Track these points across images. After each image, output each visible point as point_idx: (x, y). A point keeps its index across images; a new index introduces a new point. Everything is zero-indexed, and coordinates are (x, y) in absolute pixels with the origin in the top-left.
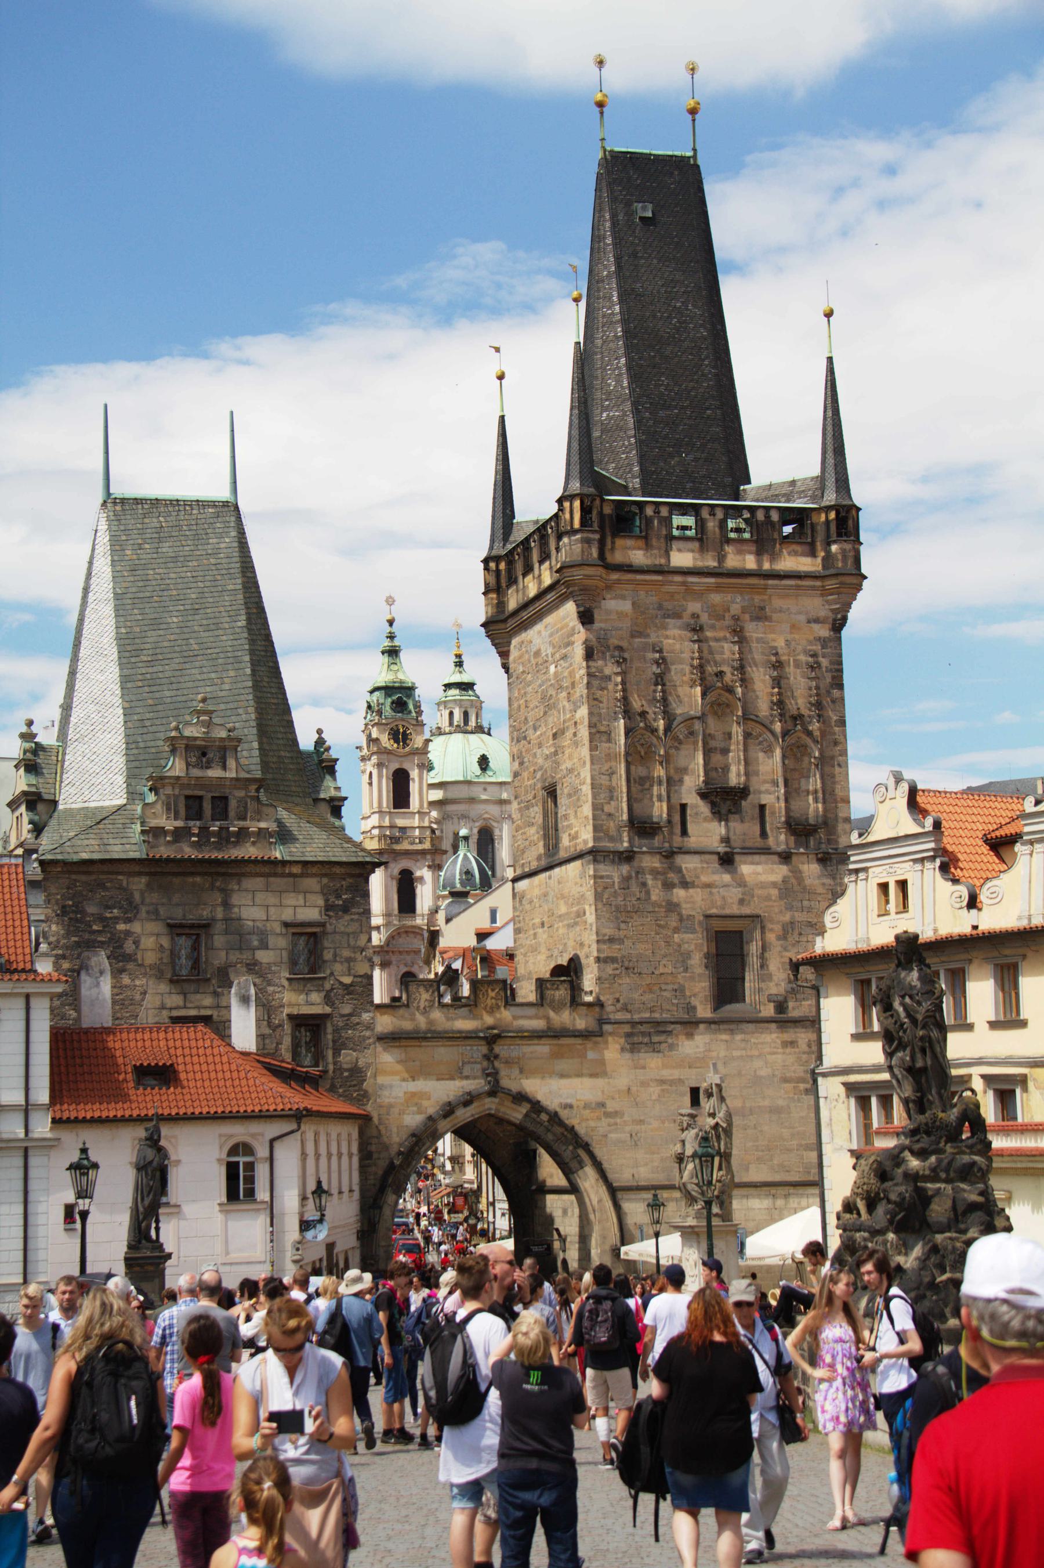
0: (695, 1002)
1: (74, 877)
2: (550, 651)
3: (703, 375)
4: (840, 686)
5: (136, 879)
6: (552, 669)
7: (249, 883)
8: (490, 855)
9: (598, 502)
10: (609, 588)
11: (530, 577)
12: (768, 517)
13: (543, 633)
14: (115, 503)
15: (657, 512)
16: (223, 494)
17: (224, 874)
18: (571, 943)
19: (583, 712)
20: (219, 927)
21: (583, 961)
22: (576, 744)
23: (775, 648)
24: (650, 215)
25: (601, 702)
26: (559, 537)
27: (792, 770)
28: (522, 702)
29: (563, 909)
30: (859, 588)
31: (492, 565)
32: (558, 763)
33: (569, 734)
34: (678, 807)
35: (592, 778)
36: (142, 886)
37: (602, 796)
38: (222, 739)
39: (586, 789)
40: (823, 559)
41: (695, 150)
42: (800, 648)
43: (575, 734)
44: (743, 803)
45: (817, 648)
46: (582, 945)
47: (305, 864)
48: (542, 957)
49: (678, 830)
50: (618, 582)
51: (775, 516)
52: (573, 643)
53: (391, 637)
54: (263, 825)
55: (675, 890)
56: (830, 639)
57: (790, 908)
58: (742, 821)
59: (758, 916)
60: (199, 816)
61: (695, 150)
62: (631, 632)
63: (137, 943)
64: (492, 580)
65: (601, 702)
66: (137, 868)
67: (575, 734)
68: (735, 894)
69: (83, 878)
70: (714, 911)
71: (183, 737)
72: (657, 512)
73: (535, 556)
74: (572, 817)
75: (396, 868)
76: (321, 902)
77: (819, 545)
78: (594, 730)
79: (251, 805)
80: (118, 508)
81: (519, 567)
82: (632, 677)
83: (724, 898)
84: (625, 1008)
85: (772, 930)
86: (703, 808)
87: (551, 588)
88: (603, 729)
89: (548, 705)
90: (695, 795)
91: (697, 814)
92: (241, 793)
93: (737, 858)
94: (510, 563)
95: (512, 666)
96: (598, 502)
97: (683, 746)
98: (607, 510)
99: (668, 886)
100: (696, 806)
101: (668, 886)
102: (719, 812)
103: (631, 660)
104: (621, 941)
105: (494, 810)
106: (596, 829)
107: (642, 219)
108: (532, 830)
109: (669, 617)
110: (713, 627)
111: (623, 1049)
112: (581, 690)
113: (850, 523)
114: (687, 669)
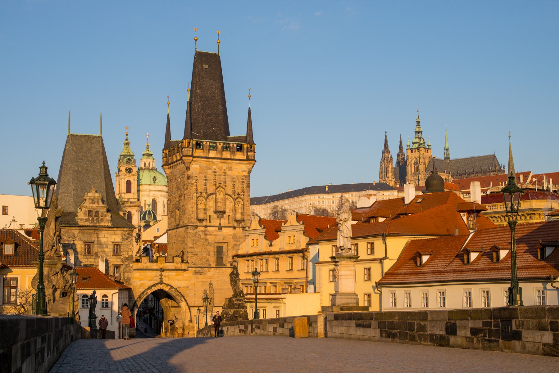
0: (211, 263)
4: (249, 187)
5: (76, 231)
6: (179, 180)
7: (103, 232)
8: (155, 205)
11: (174, 156)
12: (233, 145)
15: (206, 143)
17: (97, 230)
18: (181, 248)
20: (96, 243)
26: (182, 149)
29: (180, 239)
30: (254, 164)
31: (165, 151)
33: (183, 197)
36: (77, 232)
42: (240, 178)
43: (184, 197)
45: (244, 178)
46: (184, 248)
51: (235, 145)
56: (247, 176)
57: (235, 241)
58: (224, 219)
60: (91, 215)
68: (222, 237)
70: (216, 241)
72: (206, 143)
73: (176, 151)
74: (183, 217)
76: (121, 237)
79: (105, 213)
81: (172, 153)
82: (198, 184)
84: (194, 264)
86: (215, 216)
87: (179, 160)
92: (102, 210)
98: (194, 143)
99: (206, 235)
100: (213, 216)
101: (206, 235)
105: (158, 194)
109: (208, 169)
110: (219, 172)
111: (193, 274)
113: (253, 148)
114: (212, 182)
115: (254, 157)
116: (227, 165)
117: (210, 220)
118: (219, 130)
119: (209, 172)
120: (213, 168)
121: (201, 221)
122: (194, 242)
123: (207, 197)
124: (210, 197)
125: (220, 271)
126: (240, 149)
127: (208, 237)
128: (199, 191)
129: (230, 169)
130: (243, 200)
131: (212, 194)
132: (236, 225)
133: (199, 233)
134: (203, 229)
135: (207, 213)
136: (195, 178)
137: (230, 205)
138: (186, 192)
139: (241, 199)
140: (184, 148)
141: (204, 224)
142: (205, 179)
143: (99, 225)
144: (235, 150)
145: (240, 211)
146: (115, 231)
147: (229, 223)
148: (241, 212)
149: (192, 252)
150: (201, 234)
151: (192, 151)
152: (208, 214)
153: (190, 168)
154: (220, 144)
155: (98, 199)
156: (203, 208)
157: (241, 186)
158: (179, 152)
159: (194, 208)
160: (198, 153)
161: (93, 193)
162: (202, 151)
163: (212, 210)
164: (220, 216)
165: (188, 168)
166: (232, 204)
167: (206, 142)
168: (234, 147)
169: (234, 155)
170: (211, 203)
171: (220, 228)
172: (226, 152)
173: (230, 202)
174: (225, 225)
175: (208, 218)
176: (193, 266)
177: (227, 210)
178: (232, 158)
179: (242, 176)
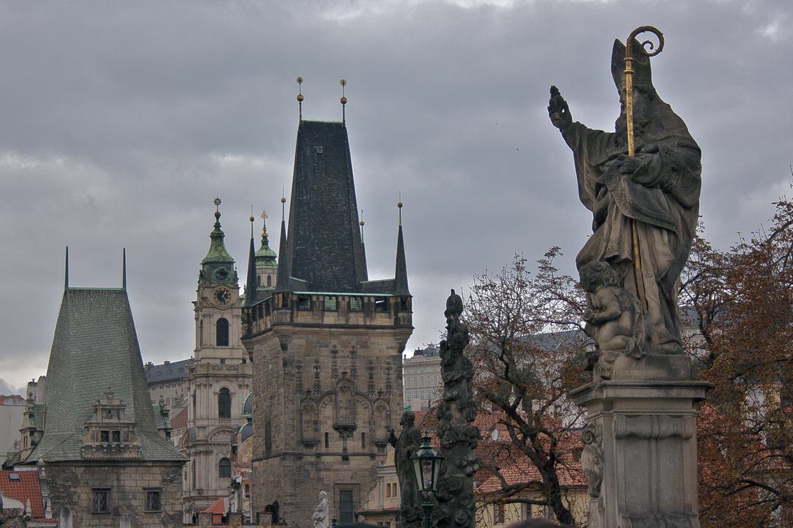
1: (52, 468)
5: (79, 468)
7: (128, 470)
10: (295, 333)
11: (261, 321)
12: (369, 300)
15: (318, 298)
16: (120, 286)
18: (275, 495)
20: (115, 489)
22: (279, 404)
23: (371, 360)
26: (273, 311)
29: (272, 479)
31: (246, 310)
33: (276, 398)
36: (81, 472)
38: (118, 406)
41: (344, 120)
44: (354, 432)
45: (391, 360)
46: (279, 496)
47: (154, 461)
49: (324, 444)
51: (373, 300)
53: (217, 226)
54: (135, 444)
56: (397, 356)
59: (359, 484)
61: (344, 120)
63: (79, 497)
64: (246, 318)
66: (79, 464)
68: (349, 474)
69: (57, 468)
71: (101, 405)
72: (318, 298)
75: (217, 387)
76: (160, 478)
80: (72, 295)
81: (258, 313)
83: (343, 476)
85: (365, 490)
86: (337, 434)
87: (270, 330)
93: (350, 458)
97: (327, 407)
98: (295, 298)
99: (319, 470)
100: (333, 433)
104: (296, 496)
106: (286, 444)
108: (261, 439)
110: (343, 351)
112: (281, 380)
113: (407, 304)
117: (327, 441)
118: (345, 270)
120: (332, 344)
121: (309, 445)
123: (320, 401)
126: (384, 307)
128: (306, 387)
129: (365, 345)
130: (388, 403)
131: (329, 393)
132: (375, 450)
133: (309, 467)
134: (313, 459)
138: (282, 390)
139: (384, 400)
141: (314, 450)
143: (119, 457)
144: (373, 309)
145: (384, 423)
146: (149, 467)
147: (363, 446)
148: (385, 425)
149: (292, 504)
150: (310, 469)
151: (292, 314)
153: (289, 347)
154: (344, 299)
155: (119, 409)
156: (313, 419)
157: (384, 377)
159: (295, 420)
160: (303, 317)
161: (108, 398)
162: (310, 313)
163: (330, 423)
164: (345, 434)
165: (284, 347)
166: (368, 412)
168: (372, 303)
169: (372, 319)
170: (327, 412)
173: (365, 408)
177: (360, 423)
178: (368, 323)
179: (388, 358)
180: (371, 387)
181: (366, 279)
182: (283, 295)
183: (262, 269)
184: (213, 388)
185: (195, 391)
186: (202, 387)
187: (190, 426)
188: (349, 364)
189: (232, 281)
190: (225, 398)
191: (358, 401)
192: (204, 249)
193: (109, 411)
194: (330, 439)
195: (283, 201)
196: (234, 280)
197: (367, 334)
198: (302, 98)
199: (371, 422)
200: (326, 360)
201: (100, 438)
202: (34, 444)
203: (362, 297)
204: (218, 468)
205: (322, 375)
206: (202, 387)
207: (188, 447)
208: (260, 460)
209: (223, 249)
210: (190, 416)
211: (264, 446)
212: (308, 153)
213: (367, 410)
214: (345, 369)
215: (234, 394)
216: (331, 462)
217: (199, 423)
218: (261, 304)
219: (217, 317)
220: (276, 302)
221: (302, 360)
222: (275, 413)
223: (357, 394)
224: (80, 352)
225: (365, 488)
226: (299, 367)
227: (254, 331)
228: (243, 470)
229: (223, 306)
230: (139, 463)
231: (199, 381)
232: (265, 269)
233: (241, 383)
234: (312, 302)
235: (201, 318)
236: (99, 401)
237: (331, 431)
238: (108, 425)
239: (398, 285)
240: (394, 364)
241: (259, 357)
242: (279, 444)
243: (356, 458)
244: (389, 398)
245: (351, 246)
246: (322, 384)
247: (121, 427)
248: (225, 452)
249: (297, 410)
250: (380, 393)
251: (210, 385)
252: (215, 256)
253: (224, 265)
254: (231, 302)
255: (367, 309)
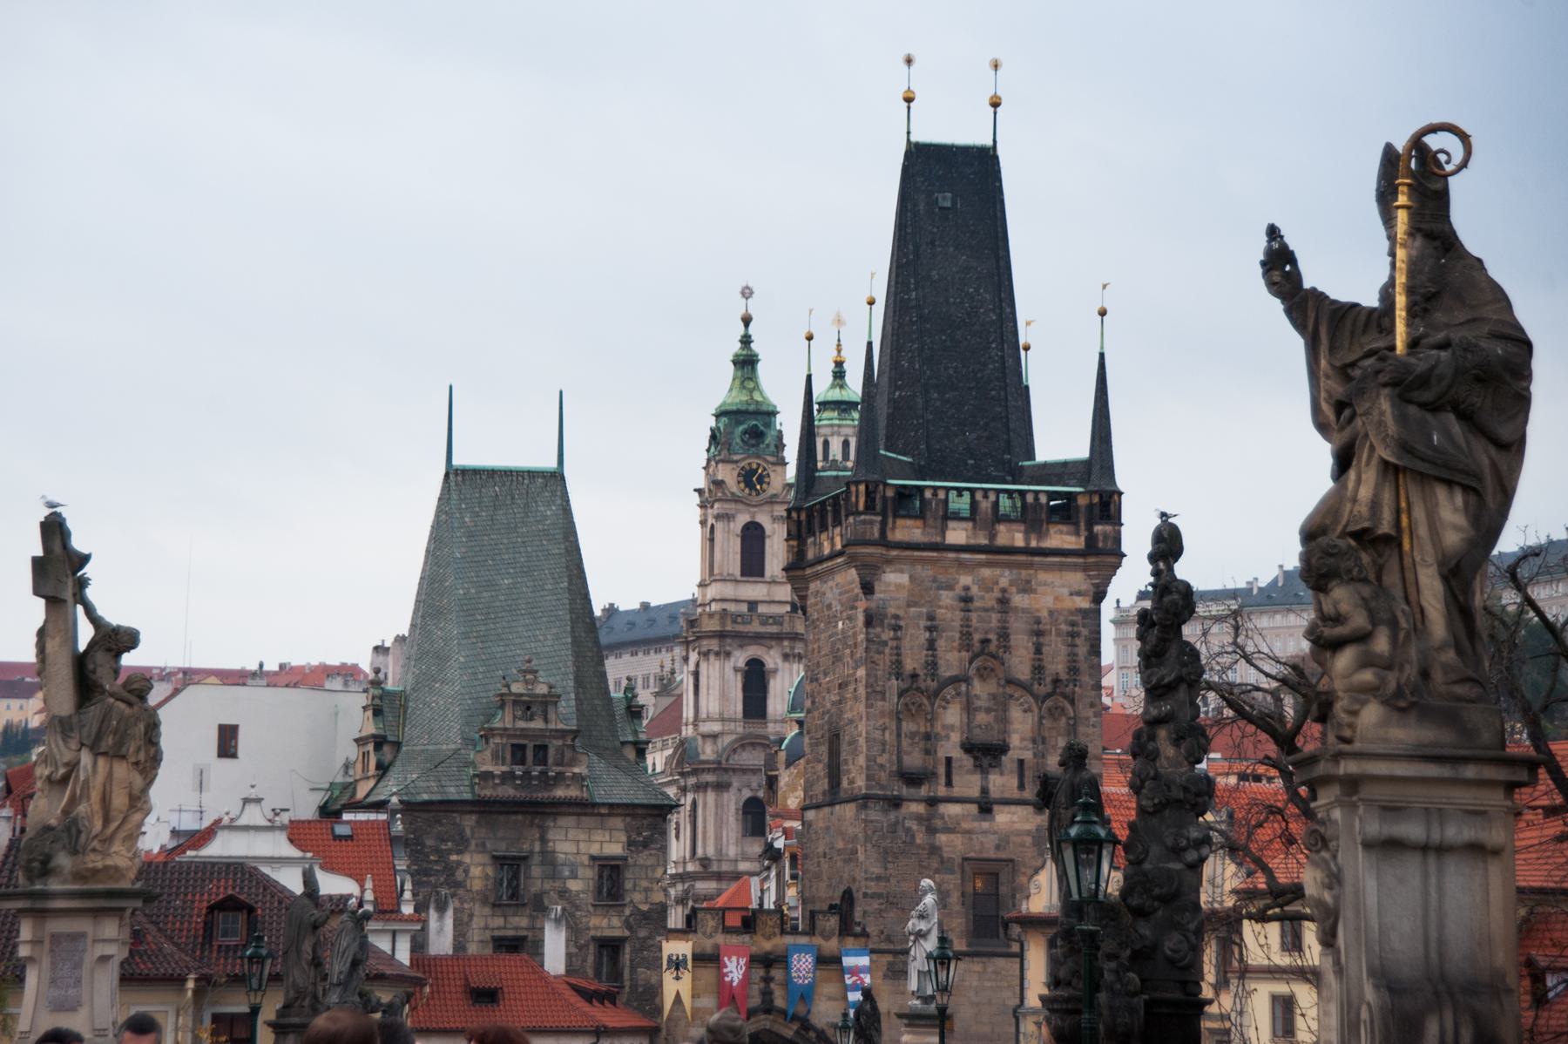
1: (416, 814)
2: (839, 608)
3: (990, 358)
5: (468, 817)
6: (840, 624)
7: (564, 821)
9: (881, 487)
10: (889, 562)
11: (824, 536)
12: (1036, 499)
13: (835, 590)
14: (456, 474)
15: (935, 494)
16: (549, 462)
17: (542, 813)
18: (846, 876)
19: (861, 672)
20: (536, 859)
21: (855, 895)
24: (948, 204)
25: (877, 665)
26: (847, 516)
27: (1050, 728)
28: (816, 646)
29: (840, 845)
30: (1119, 565)
31: (794, 515)
32: (841, 712)
33: (851, 688)
34: (944, 760)
35: (867, 733)
37: (875, 749)
38: (544, 696)
39: (862, 741)
40: (1087, 539)
42: (1061, 618)
43: (855, 690)
44: (1003, 758)
46: (854, 880)
47: (611, 806)
48: (823, 885)
49: (943, 780)
50: (898, 558)
51: (1043, 499)
52: (856, 608)
53: (746, 341)
54: (576, 770)
55: (938, 835)
59: (1012, 861)
60: (523, 762)
62: (908, 602)
63: (466, 871)
64: (794, 530)
65: (877, 665)
66: (469, 808)
67: (855, 690)
68: (991, 841)
69: (425, 815)
70: (972, 855)
71: (511, 694)
72: (935, 494)
74: (850, 762)
75: (740, 658)
76: (624, 838)
77: (1082, 525)
78: (869, 690)
80: (460, 478)
81: (817, 522)
82: (906, 643)
83: (982, 843)
84: (889, 939)
85: (1024, 873)
86: (968, 761)
87: (840, 554)
88: (878, 689)
89: (837, 659)
90: (959, 749)
91: (960, 767)
93: (996, 808)
94: (810, 517)
95: (809, 610)
96: (881, 487)
98: (890, 493)
99: (932, 831)
100: (961, 760)
101: (932, 831)
102: (981, 766)
103: (907, 627)
106: (869, 778)
107: (941, 208)
110: (982, 598)
111: (885, 976)
112: (860, 652)
113: (1112, 507)
114: (957, 635)
115: (1117, 540)
116: (1015, 572)
119: (947, 597)
121: (913, 779)
122: (886, 855)
123: (937, 693)
124: (949, 691)
125: (985, 969)
126: (1065, 512)
127: (942, 838)
128: (910, 665)
130: (1072, 702)
131: (955, 680)
133: (908, 823)
134: (919, 808)
135: (935, 752)
136: (893, 622)
137: (1021, 725)
140: (853, 514)
141: (924, 791)
142: (929, 623)
143: (546, 795)
144: (1044, 516)
146: (602, 815)
147: (1021, 786)
150: (915, 827)
151: (884, 524)
152: (942, 754)
153: (876, 588)
154: (986, 497)
156: (922, 730)
157: (1064, 650)
158: (840, 524)
160: (907, 530)
161: (527, 682)
162: (919, 523)
163: (956, 738)
164: (986, 761)
165: (868, 588)
167: (935, 489)
168: (1041, 505)
169: (1041, 535)
170: (952, 715)
171: (986, 807)
172: (1008, 525)
174: (1007, 795)
175: (942, 770)
176: (884, 946)
177: (1015, 740)
178: (1034, 544)
180: (1038, 669)
181: (1030, 453)
182: (867, 487)
183: (832, 426)
184: (733, 659)
185: (697, 665)
186: (712, 658)
187: (688, 732)
188: (994, 623)
189: (772, 448)
190: (755, 680)
191: (1011, 696)
192: (720, 387)
193: (527, 706)
194: (954, 771)
195: (871, 303)
196: (776, 447)
197: (1030, 566)
198: (912, 95)
199: (1039, 740)
200: (949, 616)
201: (508, 757)
202: (383, 769)
203: (1022, 493)
204: (740, 817)
205: (941, 644)
206: (712, 658)
207: (682, 774)
208: (817, 807)
209: (757, 387)
210: (688, 712)
211: (826, 781)
212: (922, 207)
213: (1030, 714)
214: (986, 633)
215: (775, 671)
216: (957, 816)
217: (706, 728)
218: (823, 503)
219: (743, 519)
220: (853, 499)
221: (901, 613)
222: (848, 715)
223: (1010, 682)
224: (473, 591)
225: (1023, 870)
226: (896, 628)
227: (811, 555)
228: (788, 824)
229: (755, 499)
230: (584, 808)
231: (706, 644)
232: (839, 426)
233: (788, 651)
234: (923, 500)
235: (710, 521)
236: (508, 686)
237: (957, 753)
238: (524, 733)
239: (1096, 468)
240: (1083, 627)
241: (820, 606)
242: (856, 778)
243: (1006, 808)
244: (1074, 693)
245: (1002, 393)
246: (941, 662)
247: (550, 737)
248: (754, 785)
249: (891, 712)
250: (1056, 681)
251: (728, 654)
252: (739, 399)
253: (759, 417)
254: (771, 491)
255: (1033, 517)
